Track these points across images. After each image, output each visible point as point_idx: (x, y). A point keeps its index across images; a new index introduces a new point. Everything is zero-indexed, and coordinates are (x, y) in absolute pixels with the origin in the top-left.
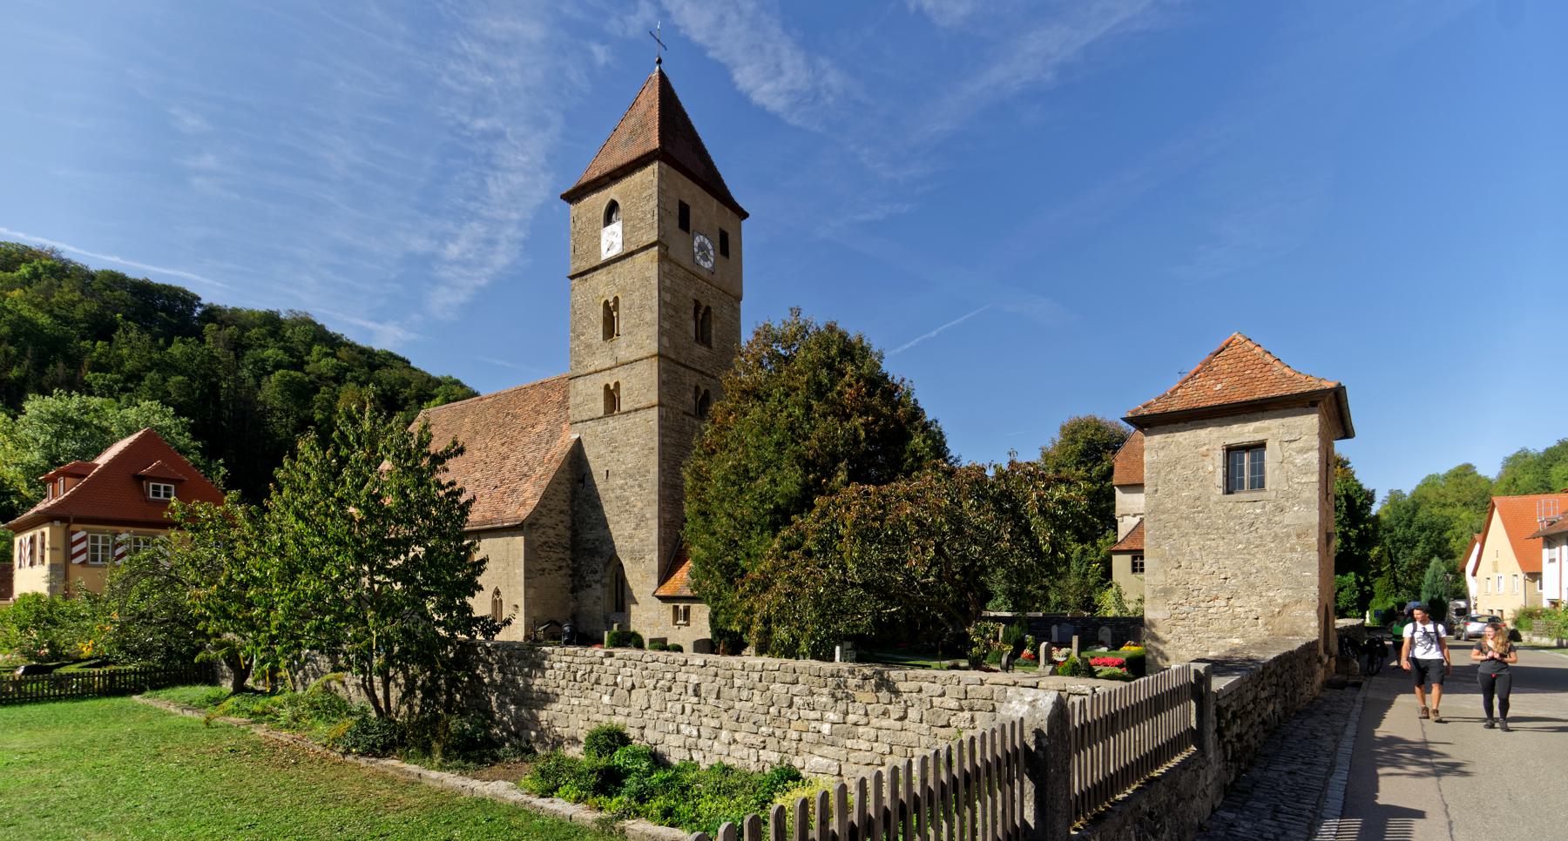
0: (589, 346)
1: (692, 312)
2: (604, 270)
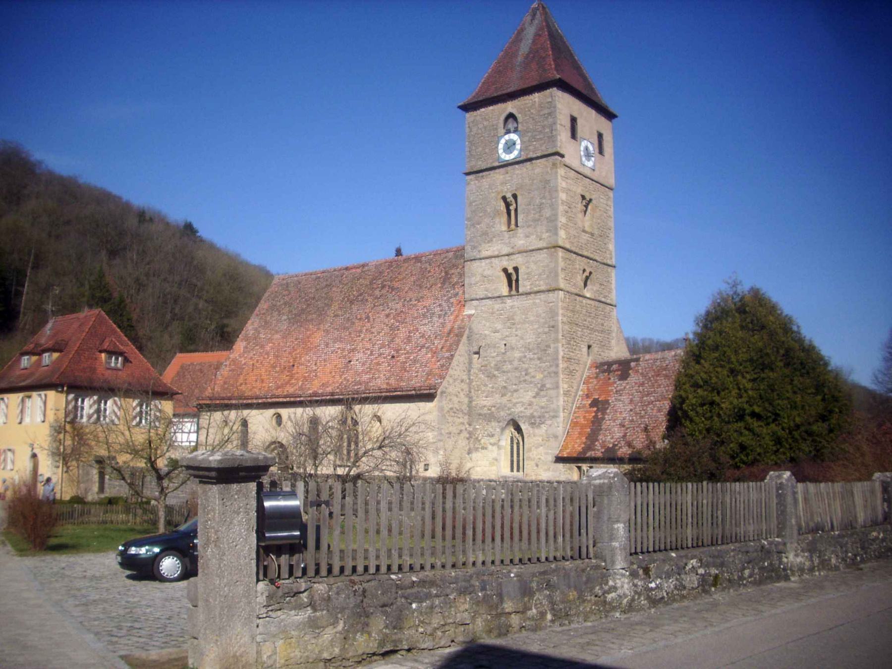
0: (485, 234)
2: (502, 170)
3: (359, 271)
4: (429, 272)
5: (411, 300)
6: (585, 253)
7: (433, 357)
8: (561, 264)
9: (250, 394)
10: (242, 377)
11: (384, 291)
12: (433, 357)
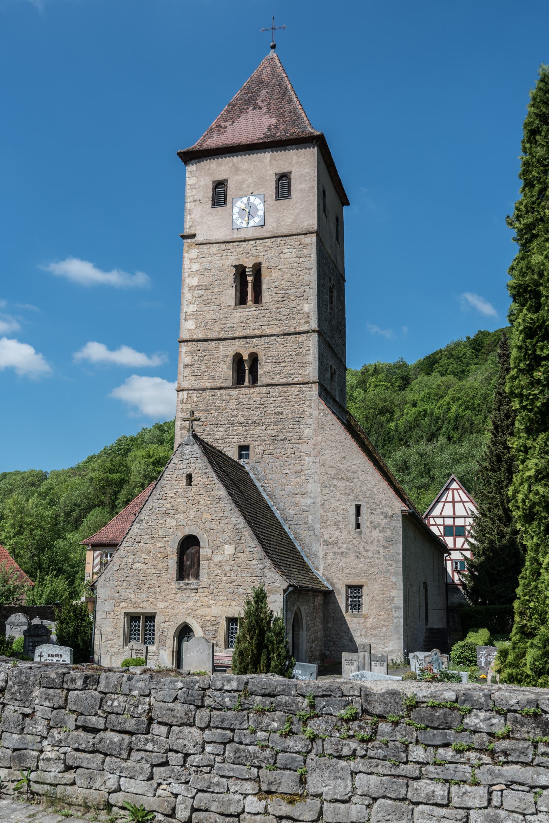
1: (230, 280)
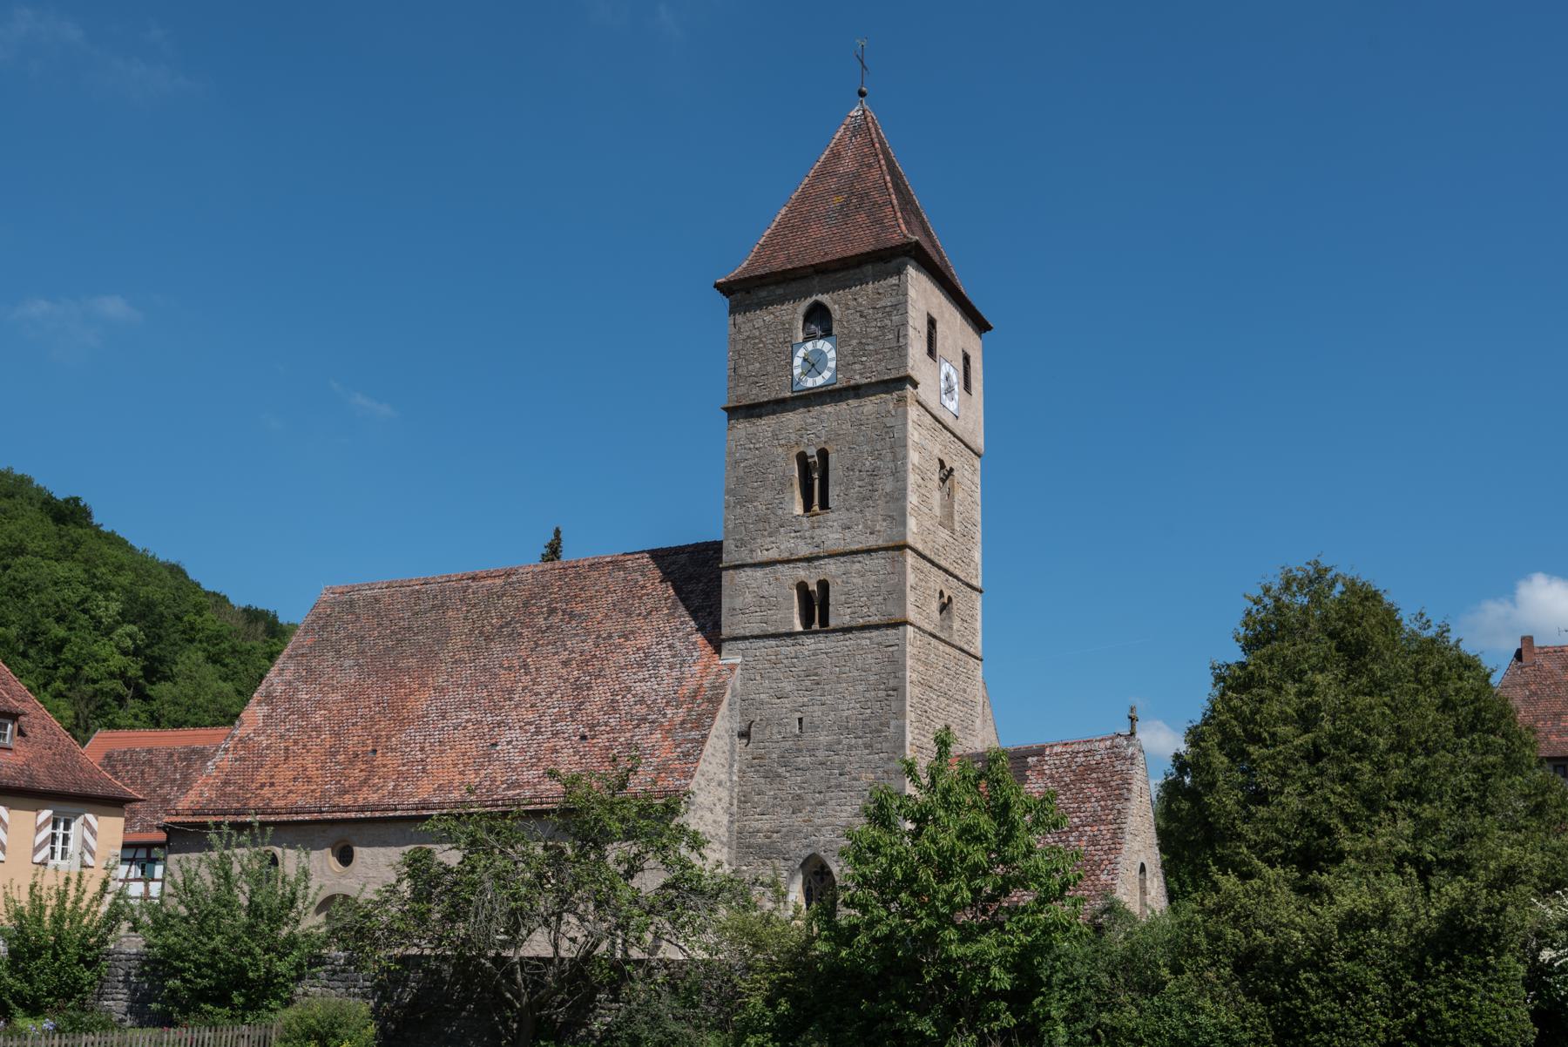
1: (936, 477)
3: (498, 582)
4: (643, 587)
5: (610, 636)
6: (943, 563)
7: (665, 739)
8: (911, 578)
9: (282, 803)
10: (262, 772)
11: (555, 620)
12: (665, 739)
